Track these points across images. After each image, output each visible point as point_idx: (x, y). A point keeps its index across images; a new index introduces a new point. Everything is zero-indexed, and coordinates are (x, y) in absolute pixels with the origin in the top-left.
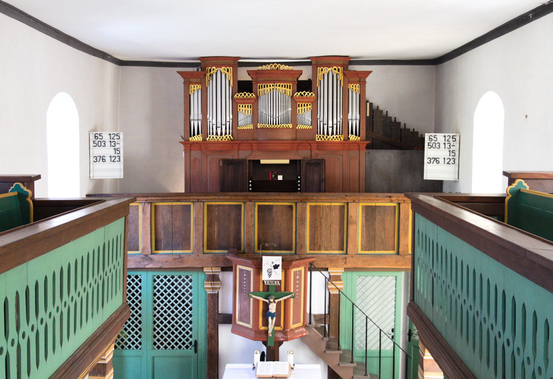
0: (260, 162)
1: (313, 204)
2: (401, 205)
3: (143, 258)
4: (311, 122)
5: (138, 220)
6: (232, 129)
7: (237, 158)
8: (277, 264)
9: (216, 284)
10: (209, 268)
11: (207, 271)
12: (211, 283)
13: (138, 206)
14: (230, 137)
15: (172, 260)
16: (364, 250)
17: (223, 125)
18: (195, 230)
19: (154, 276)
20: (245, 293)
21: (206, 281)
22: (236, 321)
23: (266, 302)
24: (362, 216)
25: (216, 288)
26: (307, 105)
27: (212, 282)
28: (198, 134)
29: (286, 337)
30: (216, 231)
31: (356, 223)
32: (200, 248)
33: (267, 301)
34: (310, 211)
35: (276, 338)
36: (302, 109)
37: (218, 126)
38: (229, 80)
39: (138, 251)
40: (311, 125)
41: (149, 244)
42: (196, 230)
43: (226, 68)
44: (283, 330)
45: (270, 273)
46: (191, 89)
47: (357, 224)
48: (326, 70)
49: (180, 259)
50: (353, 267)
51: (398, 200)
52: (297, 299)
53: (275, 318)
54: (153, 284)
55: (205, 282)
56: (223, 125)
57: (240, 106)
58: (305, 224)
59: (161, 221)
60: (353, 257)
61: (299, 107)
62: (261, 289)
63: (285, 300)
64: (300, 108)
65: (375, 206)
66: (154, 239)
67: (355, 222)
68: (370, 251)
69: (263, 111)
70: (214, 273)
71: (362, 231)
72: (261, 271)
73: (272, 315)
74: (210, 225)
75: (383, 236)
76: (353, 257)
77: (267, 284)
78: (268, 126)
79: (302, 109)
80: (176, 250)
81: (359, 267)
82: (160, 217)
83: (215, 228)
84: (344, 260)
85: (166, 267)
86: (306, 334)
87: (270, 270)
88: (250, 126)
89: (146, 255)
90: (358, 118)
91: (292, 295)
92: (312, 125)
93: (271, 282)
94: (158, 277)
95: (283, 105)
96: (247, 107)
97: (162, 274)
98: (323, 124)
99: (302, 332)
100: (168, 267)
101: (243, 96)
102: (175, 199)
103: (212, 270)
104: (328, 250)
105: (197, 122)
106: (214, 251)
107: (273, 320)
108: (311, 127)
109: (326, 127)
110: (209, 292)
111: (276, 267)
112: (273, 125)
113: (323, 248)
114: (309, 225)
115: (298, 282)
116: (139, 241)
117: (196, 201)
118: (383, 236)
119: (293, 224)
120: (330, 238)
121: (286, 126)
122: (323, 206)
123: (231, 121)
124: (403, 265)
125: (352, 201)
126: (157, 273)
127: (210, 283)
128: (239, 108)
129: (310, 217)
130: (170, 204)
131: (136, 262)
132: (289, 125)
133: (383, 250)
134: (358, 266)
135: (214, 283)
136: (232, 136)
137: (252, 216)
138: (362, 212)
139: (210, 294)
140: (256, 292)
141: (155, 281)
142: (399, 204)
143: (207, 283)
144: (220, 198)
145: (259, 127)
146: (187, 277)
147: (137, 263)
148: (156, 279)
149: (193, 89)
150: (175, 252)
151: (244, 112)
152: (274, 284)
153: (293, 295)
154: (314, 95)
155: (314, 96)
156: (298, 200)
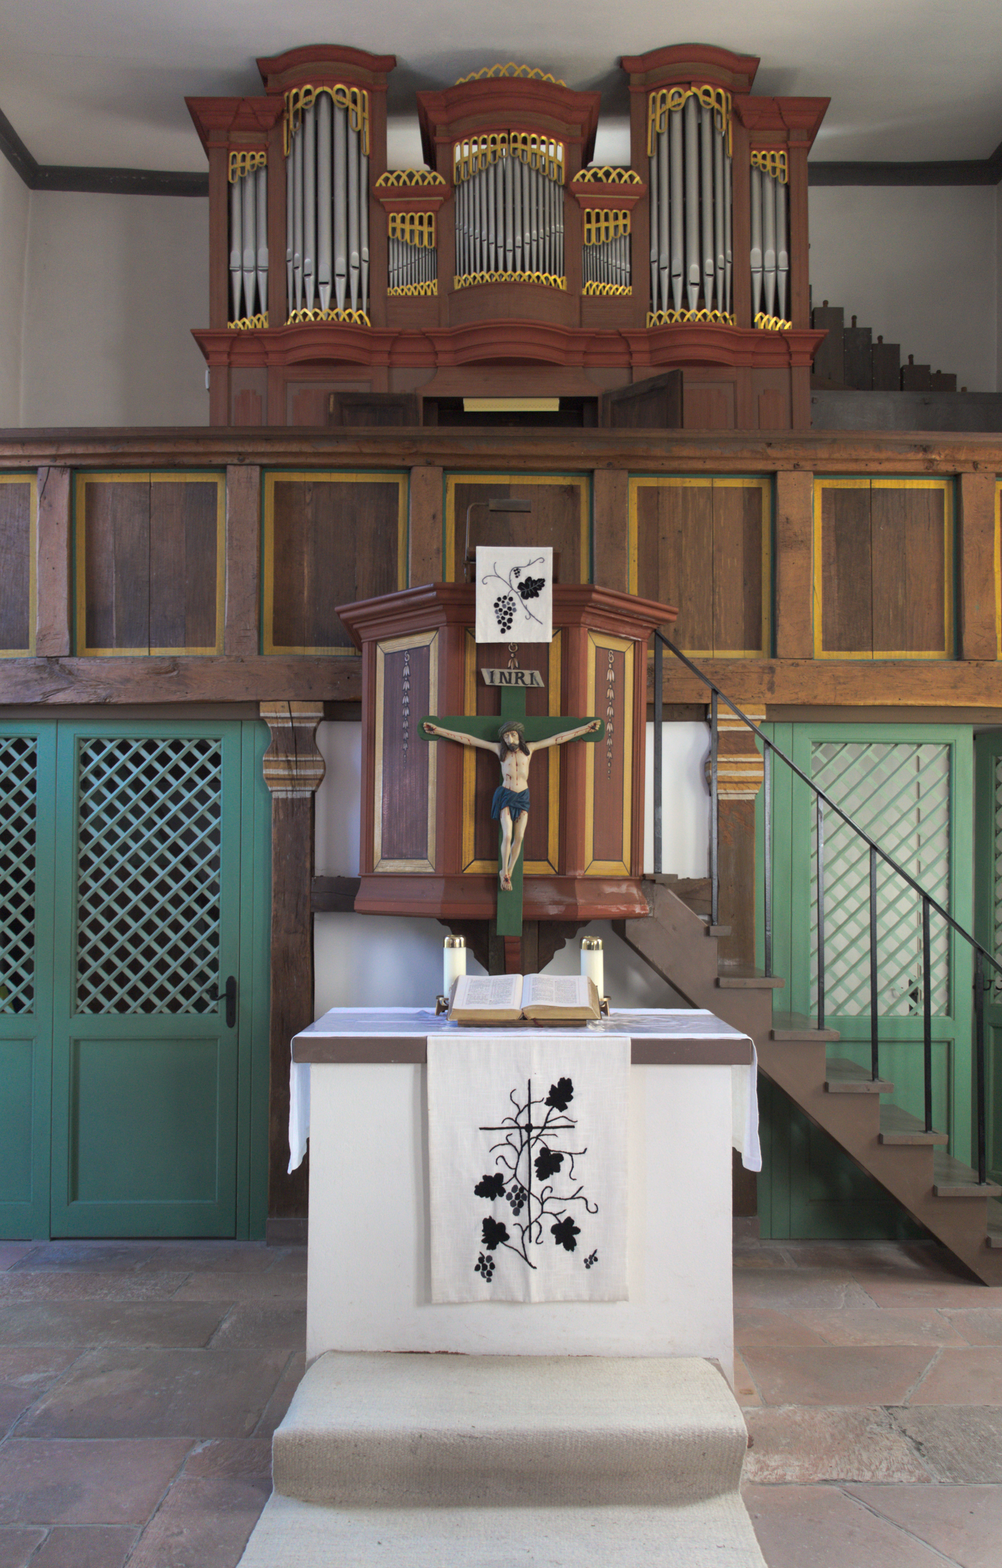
0: (462, 406)
1: (651, 482)
2: (966, 481)
3: (38, 668)
4: (628, 275)
5: (28, 538)
6: (368, 296)
7: (384, 390)
8: (535, 578)
9: (306, 764)
10: (281, 703)
11: (273, 715)
12: (289, 761)
13: (29, 484)
14: (361, 317)
15: (148, 674)
16: (833, 649)
17: (339, 275)
18: (230, 567)
19: (83, 743)
20: (405, 741)
21: (268, 753)
22: (376, 862)
23: (489, 753)
24: (823, 527)
25: (305, 779)
26: (616, 217)
27: (292, 758)
28: (257, 310)
29: (569, 900)
30: (306, 578)
31: (806, 543)
32: (249, 634)
33: (495, 748)
34: (638, 509)
35: (528, 904)
36: (598, 230)
37: (321, 279)
38: (357, 130)
39: (26, 651)
40: (631, 284)
41: (63, 616)
42: (235, 567)
43: (349, 89)
44: (558, 873)
45: (506, 613)
46: (235, 166)
47: (809, 549)
48: (674, 97)
49: (175, 673)
50: (799, 702)
51: (954, 461)
52: (610, 760)
53: (525, 817)
54: (80, 773)
55: (264, 759)
56: (339, 275)
57: (394, 219)
58: (624, 548)
59: (108, 542)
60: (797, 665)
61: (589, 221)
62: (470, 709)
63: (564, 747)
64: (593, 226)
65: (871, 489)
66: (84, 605)
67: (802, 541)
68: (855, 650)
69: (471, 229)
70: (296, 725)
71: (826, 580)
72: (469, 635)
73: (516, 803)
74: (285, 556)
75: (900, 596)
76: (797, 665)
77: (492, 681)
78: (487, 277)
79: (598, 230)
80: (163, 645)
81: (821, 702)
82: (104, 526)
83: (301, 565)
84: (766, 678)
85: (123, 699)
86: (643, 909)
87: (507, 601)
88: (429, 286)
89: (53, 660)
90: (783, 265)
91: (593, 728)
92: (633, 282)
93: (507, 675)
94: (98, 747)
95: (537, 211)
96: (417, 221)
97: (110, 732)
98: (671, 277)
99: (628, 899)
100: (131, 701)
101: (405, 183)
102: (158, 451)
103: (290, 712)
104: (707, 648)
105: (253, 274)
106: (298, 650)
107: (517, 825)
108: (628, 290)
109: (678, 282)
110: (281, 792)
111: (530, 588)
112: (503, 273)
113: (687, 639)
114: (636, 557)
115: (610, 694)
116: (28, 612)
117: (236, 461)
118: (900, 596)
119: (579, 555)
120: (713, 604)
121: (547, 278)
122: (685, 489)
123: (365, 266)
124: (979, 694)
125: (790, 467)
126: (93, 731)
127: (284, 759)
128: (391, 225)
129: (639, 527)
130: (143, 478)
131: (16, 684)
132: (559, 281)
133: (902, 650)
134: (815, 697)
135: (298, 759)
136: (368, 314)
137: (434, 517)
138: (823, 512)
139: (285, 801)
140: (452, 715)
141: (85, 760)
142: (955, 478)
143: (271, 759)
144: (322, 450)
145: (457, 287)
146: (203, 747)
147: (18, 687)
148: (91, 753)
149: (239, 163)
150: (157, 652)
151: (407, 236)
152: (520, 684)
153: (597, 728)
154: (637, 179)
155: (637, 183)
156: (597, 459)
